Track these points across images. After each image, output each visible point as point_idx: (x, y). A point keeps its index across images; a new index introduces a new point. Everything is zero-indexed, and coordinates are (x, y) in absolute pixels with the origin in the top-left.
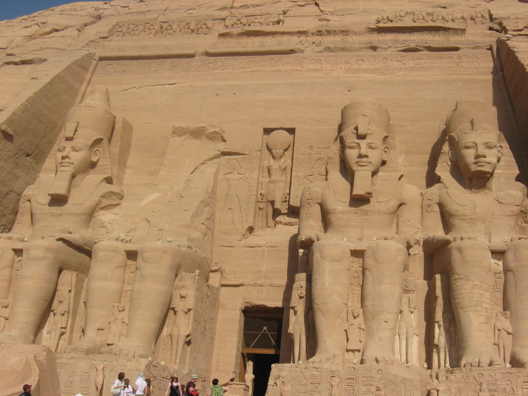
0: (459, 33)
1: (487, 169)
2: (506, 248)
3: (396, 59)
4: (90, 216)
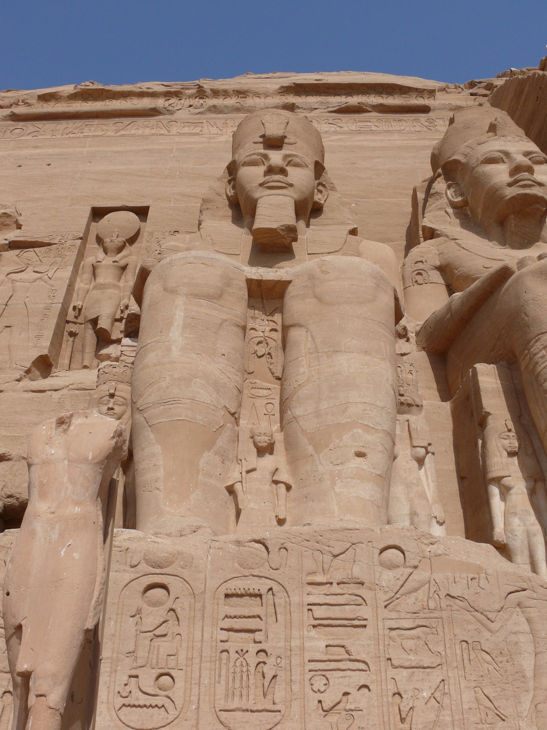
0: (426, 96)
3: (326, 121)
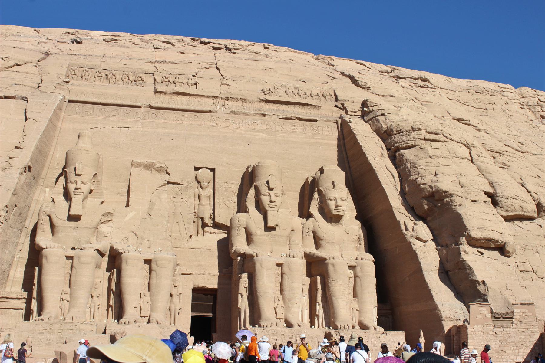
4: (96, 228)
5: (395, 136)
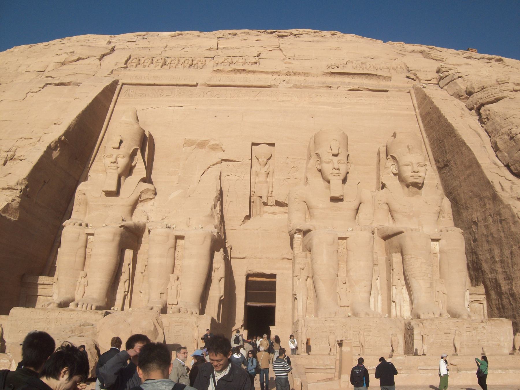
1: (419, 181)
2: (440, 237)
5: (477, 93)
